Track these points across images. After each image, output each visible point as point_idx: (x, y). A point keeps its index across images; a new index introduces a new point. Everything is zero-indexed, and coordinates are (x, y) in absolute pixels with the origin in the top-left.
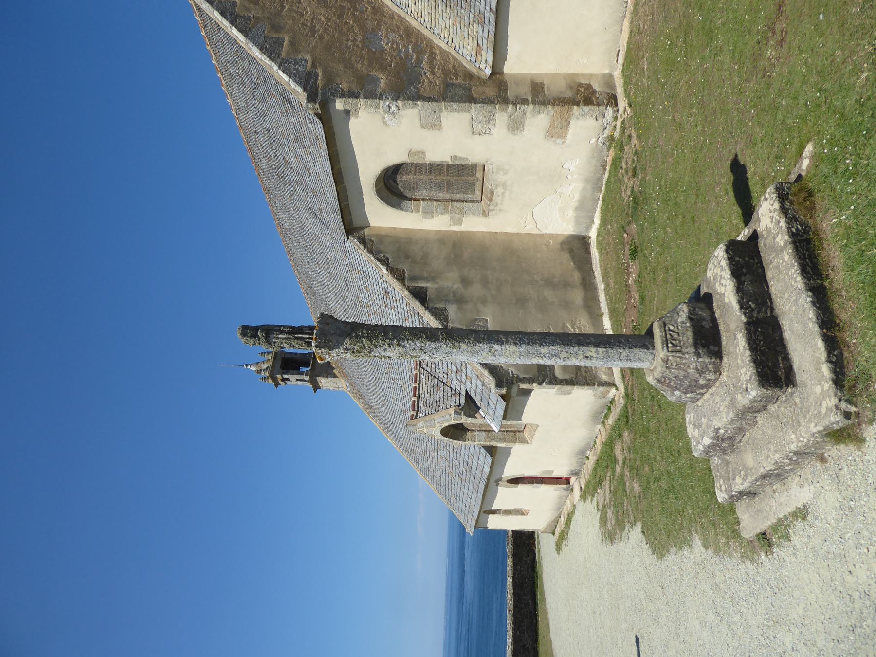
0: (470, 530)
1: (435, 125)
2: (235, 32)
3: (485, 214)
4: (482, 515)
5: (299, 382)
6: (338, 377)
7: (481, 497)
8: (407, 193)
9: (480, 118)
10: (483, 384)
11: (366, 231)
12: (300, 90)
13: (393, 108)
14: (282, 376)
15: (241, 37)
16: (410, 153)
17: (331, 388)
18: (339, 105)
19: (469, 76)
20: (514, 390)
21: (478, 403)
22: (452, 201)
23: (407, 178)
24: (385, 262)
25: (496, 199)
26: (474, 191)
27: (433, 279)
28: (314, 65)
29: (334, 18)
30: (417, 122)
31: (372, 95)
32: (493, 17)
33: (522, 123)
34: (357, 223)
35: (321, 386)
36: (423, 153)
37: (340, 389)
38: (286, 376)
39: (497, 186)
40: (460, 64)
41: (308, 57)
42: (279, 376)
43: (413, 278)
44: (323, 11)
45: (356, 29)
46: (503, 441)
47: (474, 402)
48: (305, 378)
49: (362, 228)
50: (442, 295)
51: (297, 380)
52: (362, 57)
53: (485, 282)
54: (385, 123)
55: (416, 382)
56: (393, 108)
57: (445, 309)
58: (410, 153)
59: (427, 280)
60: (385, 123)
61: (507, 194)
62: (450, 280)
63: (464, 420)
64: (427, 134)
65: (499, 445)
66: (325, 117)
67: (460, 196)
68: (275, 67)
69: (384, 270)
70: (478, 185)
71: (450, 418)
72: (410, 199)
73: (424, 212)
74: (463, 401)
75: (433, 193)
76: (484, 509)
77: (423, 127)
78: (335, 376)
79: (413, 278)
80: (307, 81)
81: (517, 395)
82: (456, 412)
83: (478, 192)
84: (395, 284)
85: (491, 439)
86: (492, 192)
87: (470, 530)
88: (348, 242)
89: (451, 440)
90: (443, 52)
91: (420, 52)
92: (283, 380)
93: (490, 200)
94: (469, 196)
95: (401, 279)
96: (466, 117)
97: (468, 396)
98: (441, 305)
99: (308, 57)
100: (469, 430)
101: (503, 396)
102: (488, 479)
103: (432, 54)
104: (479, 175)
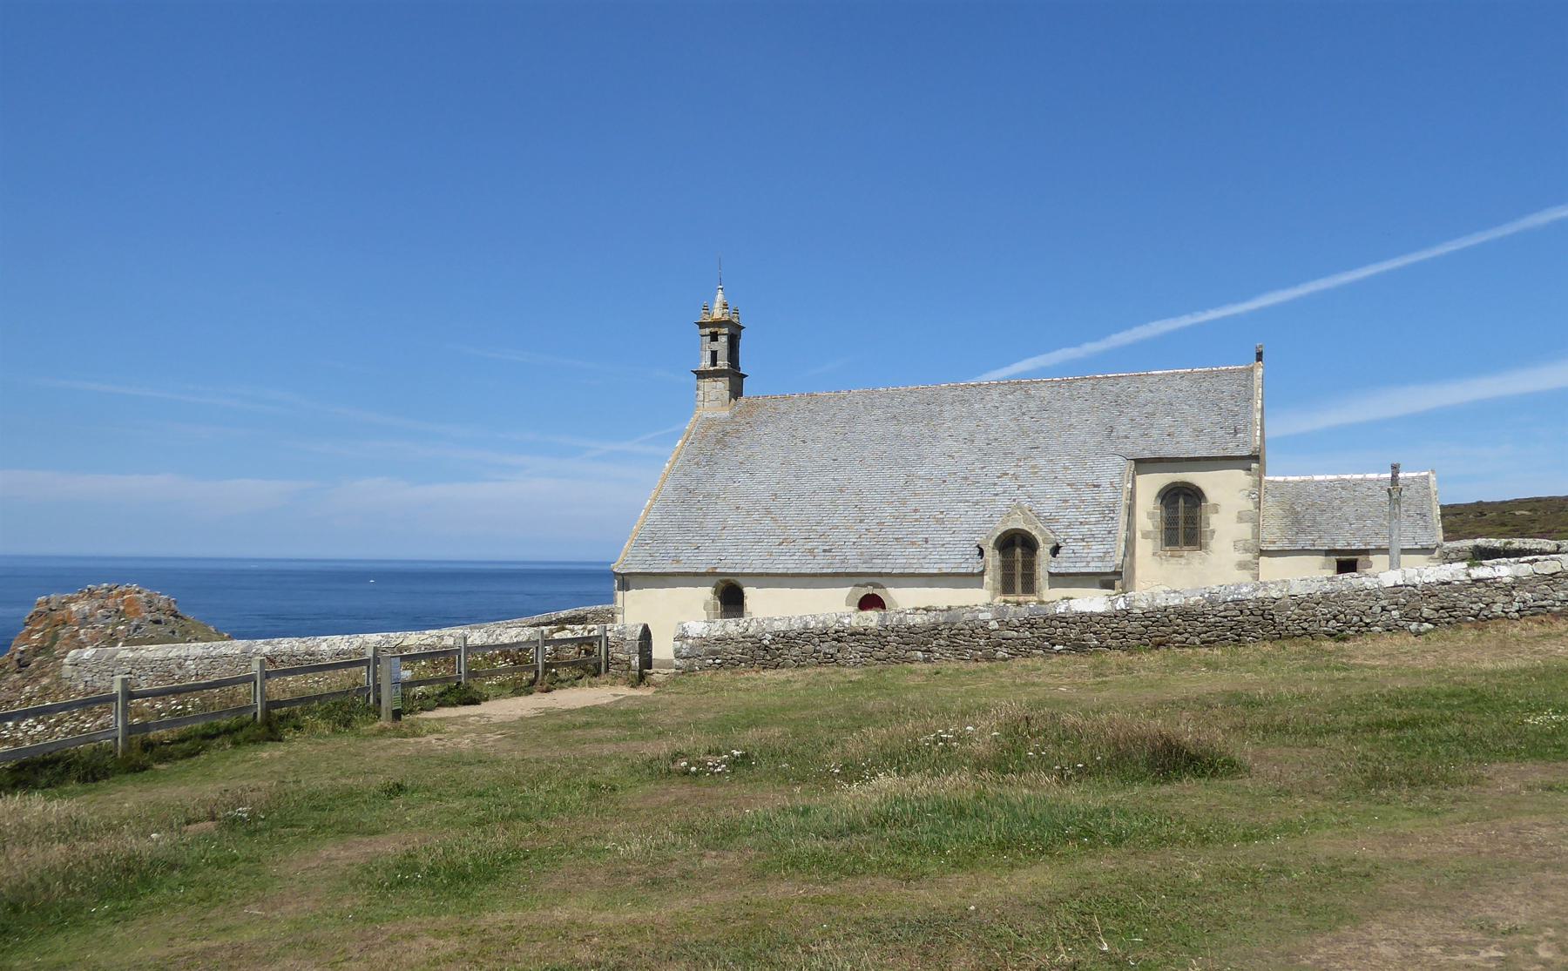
3: (1154, 554)
4: (716, 580)
5: (708, 354)
8: (1164, 502)
9: (1248, 545)
17: (701, 393)
25: (1173, 560)
33: (1244, 569)
35: (707, 380)
36: (1217, 512)
37: (700, 404)
39: (1188, 559)
42: (726, 331)
54: (1242, 490)
56: (1253, 496)
61: (1179, 566)
64: (1234, 515)
73: (1153, 513)
76: (740, 580)
77: (1239, 512)
81: (1102, 580)
86: (1181, 556)
89: (994, 538)
92: (714, 337)
94: (1164, 545)
102: (880, 575)
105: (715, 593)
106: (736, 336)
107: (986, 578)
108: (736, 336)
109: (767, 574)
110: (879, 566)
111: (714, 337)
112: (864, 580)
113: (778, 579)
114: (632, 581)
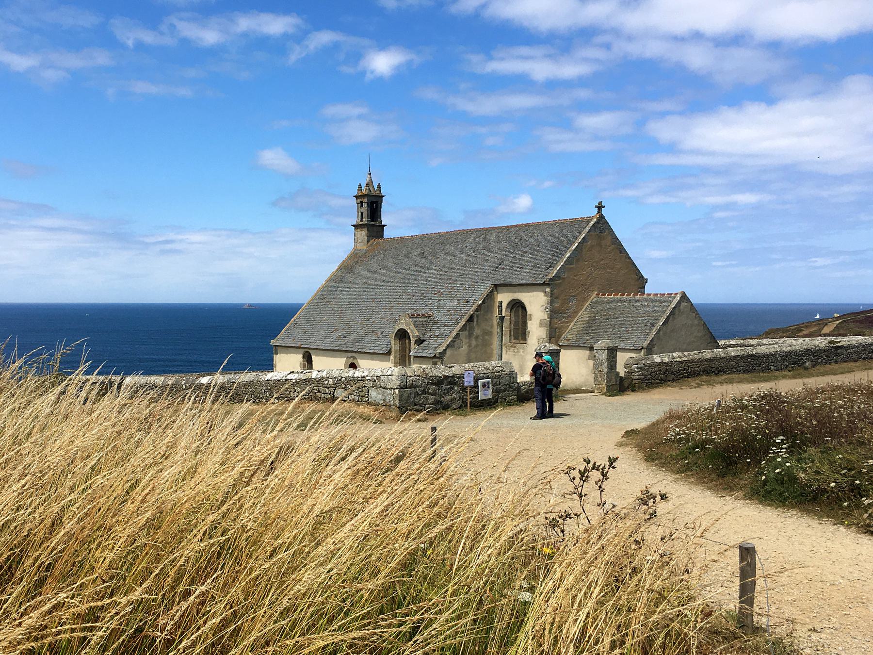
0: (273, 342)
1: (541, 325)
2: (576, 244)
4: (303, 351)
6: (367, 243)
7: (337, 348)
8: (513, 311)
10: (436, 347)
11: (495, 293)
12: (553, 275)
13: (547, 310)
14: (365, 203)
15: (574, 247)
16: (530, 315)
18: (548, 290)
19: (559, 337)
20: (437, 360)
21: (421, 345)
22: (510, 331)
23: (520, 313)
24: (483, 302)
26: (514, 339)
27: (477, 324)
28: (563, 278)
29: (581, 283)
30: (542, 318)
31: (552, 302)
32: (577, 345)
34: (499, 288)
36: (531, 320)
38: (365, 205)
40: (564, 333)
41: (566, 276)
42: (366, 200)
43: (477, 316)
44: (585, 278)
45: (577, 292)
46: (395, 357)
47: (421, 343)
48: (364, 219)
49: (497, 291)
50: (471, 329)
51: (362, 214)
52: (566, 296)
53: (476, 346)
54: (542, 306)
55: (423, 315)
56: (547, 310)
57: (466, 330)
58: (530, 315)
59: (477, 322)
60: (542, 306)
62: (477, 331)
63: (413, 340)
64: (538, 322)
65: (391, 356)
66: (544, 284)
67: (512, 333)
68: (562, 264)
69: (480, 302)
70: (518, 341)
71: (413, 333)
72: (510, 312)
74: (422, 339)
75: (513, 323)
76: (310, 351)
77: (541, 320)
78: (368, 242)
79: (477, 316)
80: (557, 277)
82: (417, 336)
83: (514, 341)
84: (474, 307)
85: (396, 352)
86: (515, 347)
87: (273, 342)
88: (489, 283)
90: (568, 326)
91: (569, 317)
92: (362, 203)
93: (511, 347)
95: (477, 310)
96: (545, 337)
97: (424, 341)
98: (468, 329)
99: (566, 276)
100: (400, 340)
101: (435, 355)
102: (355, 352)
103: (567, 322)
104: (521, 342)
105: (303, 358)
106: (376, 203)
107: (392, 357)
108: (376, 203)
109: (317, 349)
110: (359, 347)
111: (362, 203)
112: (350, 355)
113: (322, 352)
114: (279, 349)
